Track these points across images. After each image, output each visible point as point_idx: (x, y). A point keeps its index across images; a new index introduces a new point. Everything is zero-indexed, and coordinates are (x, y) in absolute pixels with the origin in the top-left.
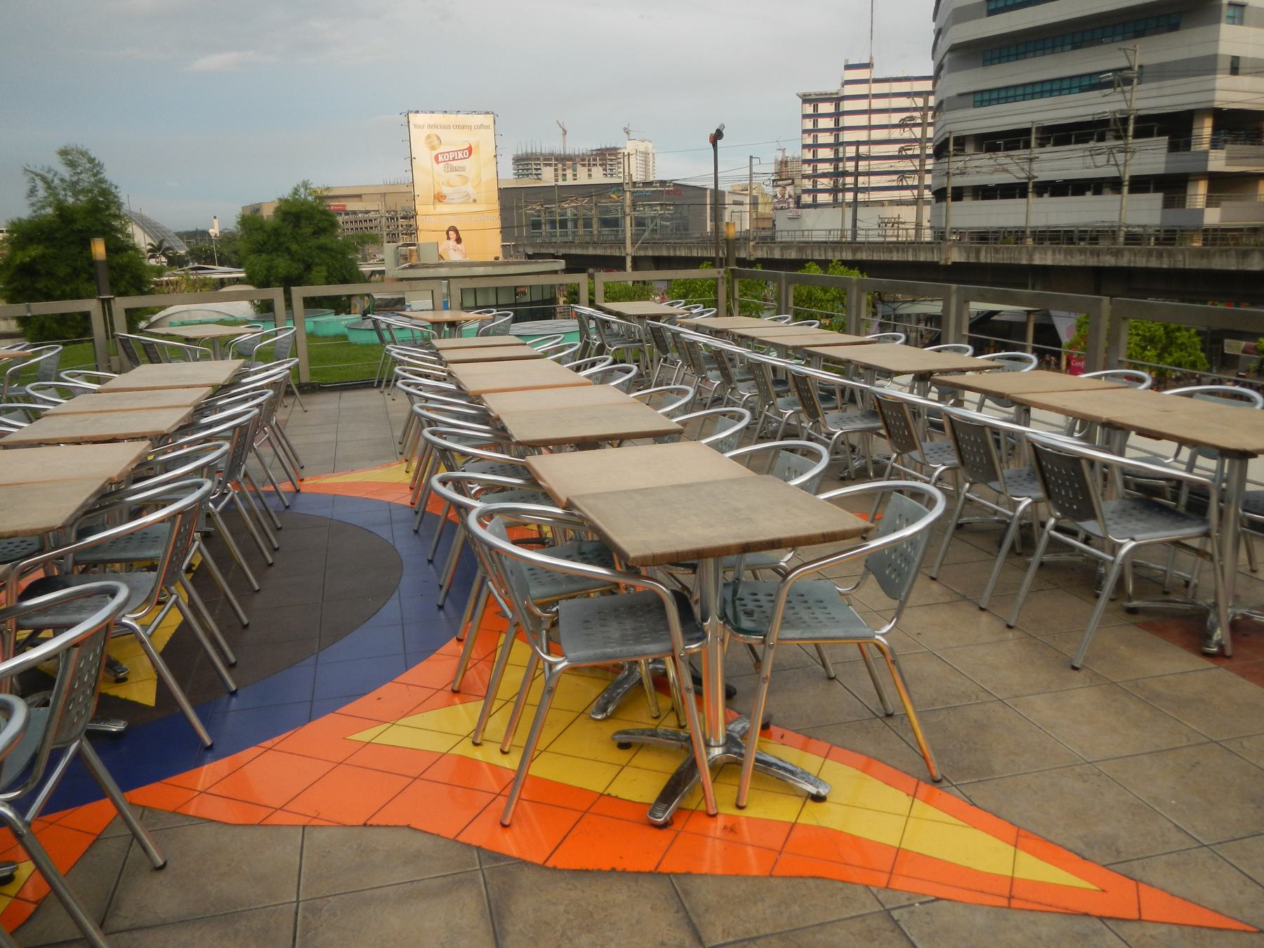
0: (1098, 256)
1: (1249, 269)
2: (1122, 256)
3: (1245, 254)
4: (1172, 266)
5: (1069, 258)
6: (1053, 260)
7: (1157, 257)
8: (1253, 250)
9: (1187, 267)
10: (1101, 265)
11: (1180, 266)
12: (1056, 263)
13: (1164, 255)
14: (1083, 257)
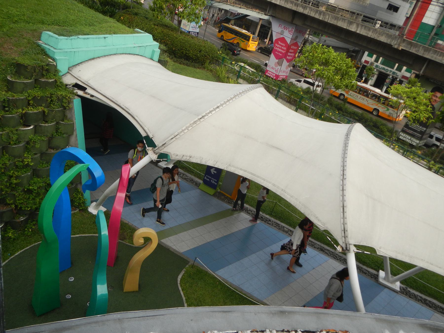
0: (297, 6)
1: (350, 29)
2: (306, 9)
3: (351, 23)
4: (323, 20)
5: (286, 3)
6: (280, 3)
7: (319, 14)
8: (354, 22)
9: (329, 22)
10: (297, 11)
11: (326, 20)
12: (280, 4)
13: (322, 14)
14: (291, 5)
